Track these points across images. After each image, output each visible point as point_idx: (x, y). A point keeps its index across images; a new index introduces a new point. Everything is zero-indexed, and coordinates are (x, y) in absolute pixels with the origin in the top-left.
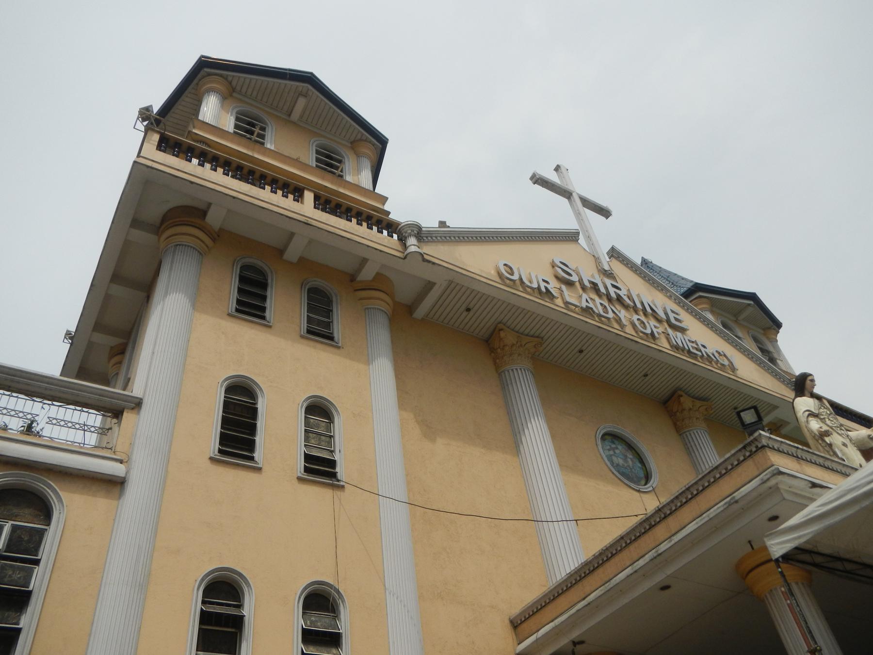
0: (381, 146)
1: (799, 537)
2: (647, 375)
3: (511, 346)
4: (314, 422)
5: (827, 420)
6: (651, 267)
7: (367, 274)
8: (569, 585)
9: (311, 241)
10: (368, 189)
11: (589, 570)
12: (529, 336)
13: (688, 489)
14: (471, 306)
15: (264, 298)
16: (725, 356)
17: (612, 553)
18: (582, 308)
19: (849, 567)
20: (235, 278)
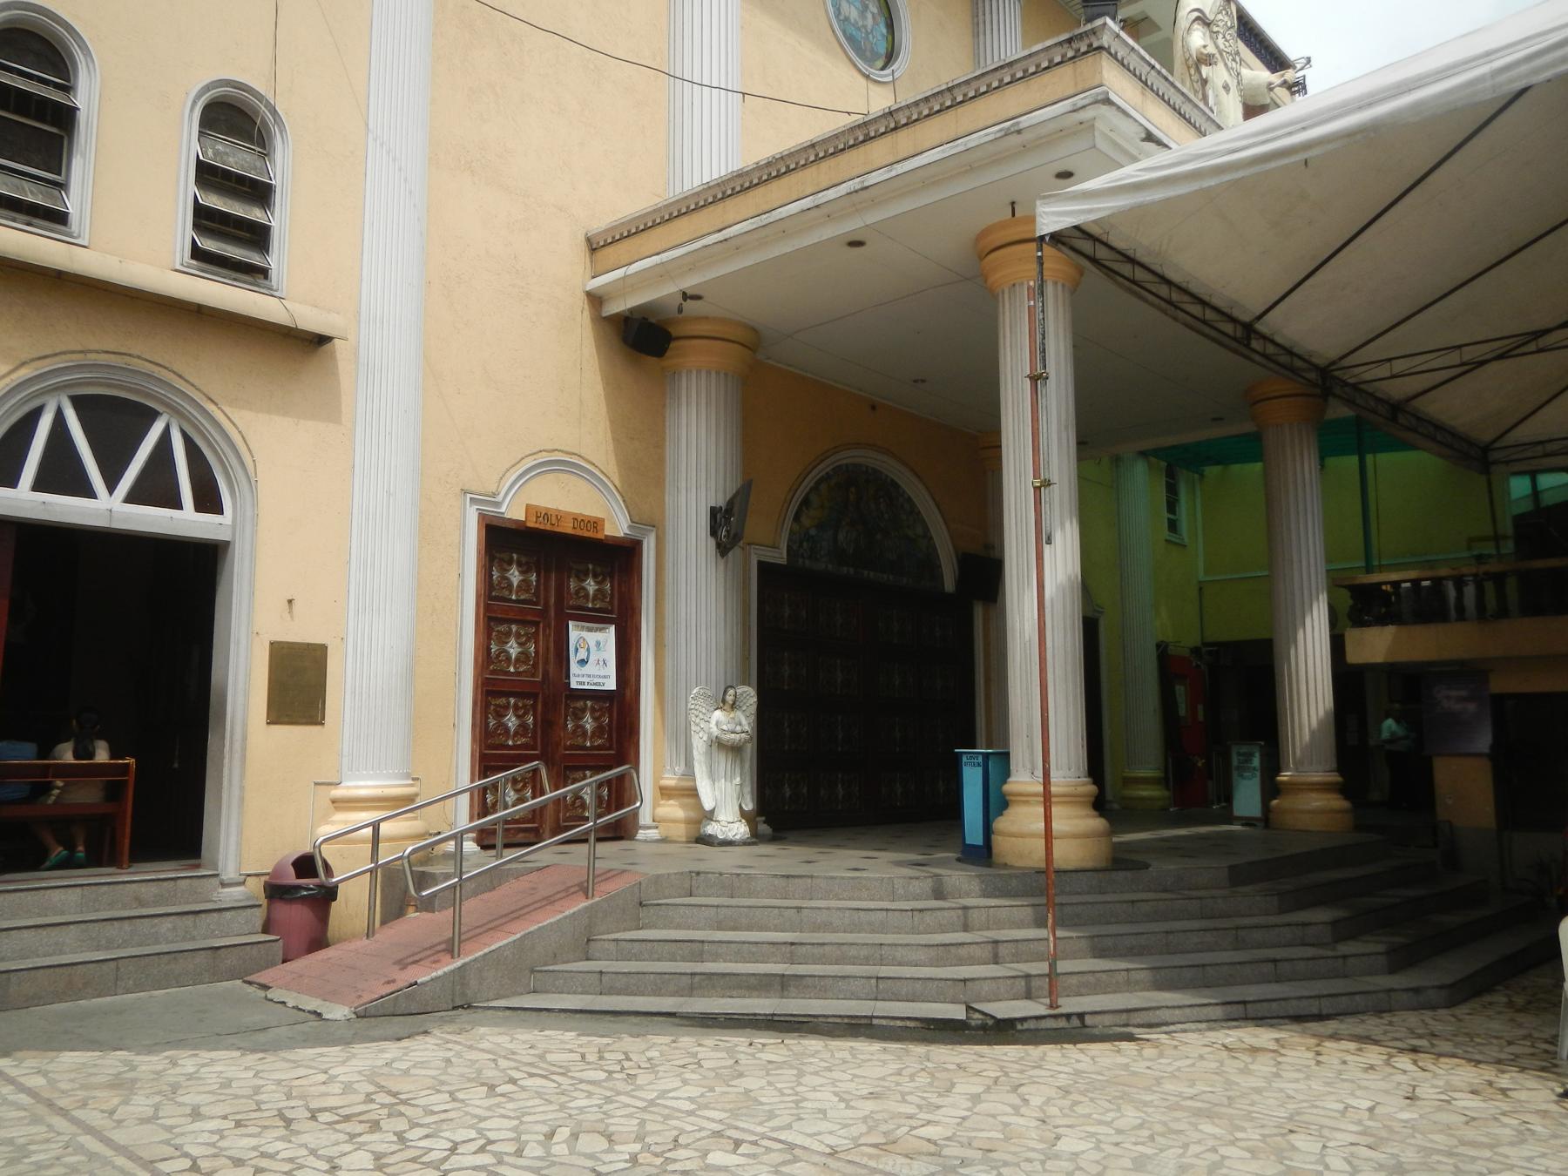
1: (1090, 211)
5: (1220, 36)
8: (702, 203)
11: (742, 186)
13: (950, 89)
17: (788, 167)
19: (1140, 275)
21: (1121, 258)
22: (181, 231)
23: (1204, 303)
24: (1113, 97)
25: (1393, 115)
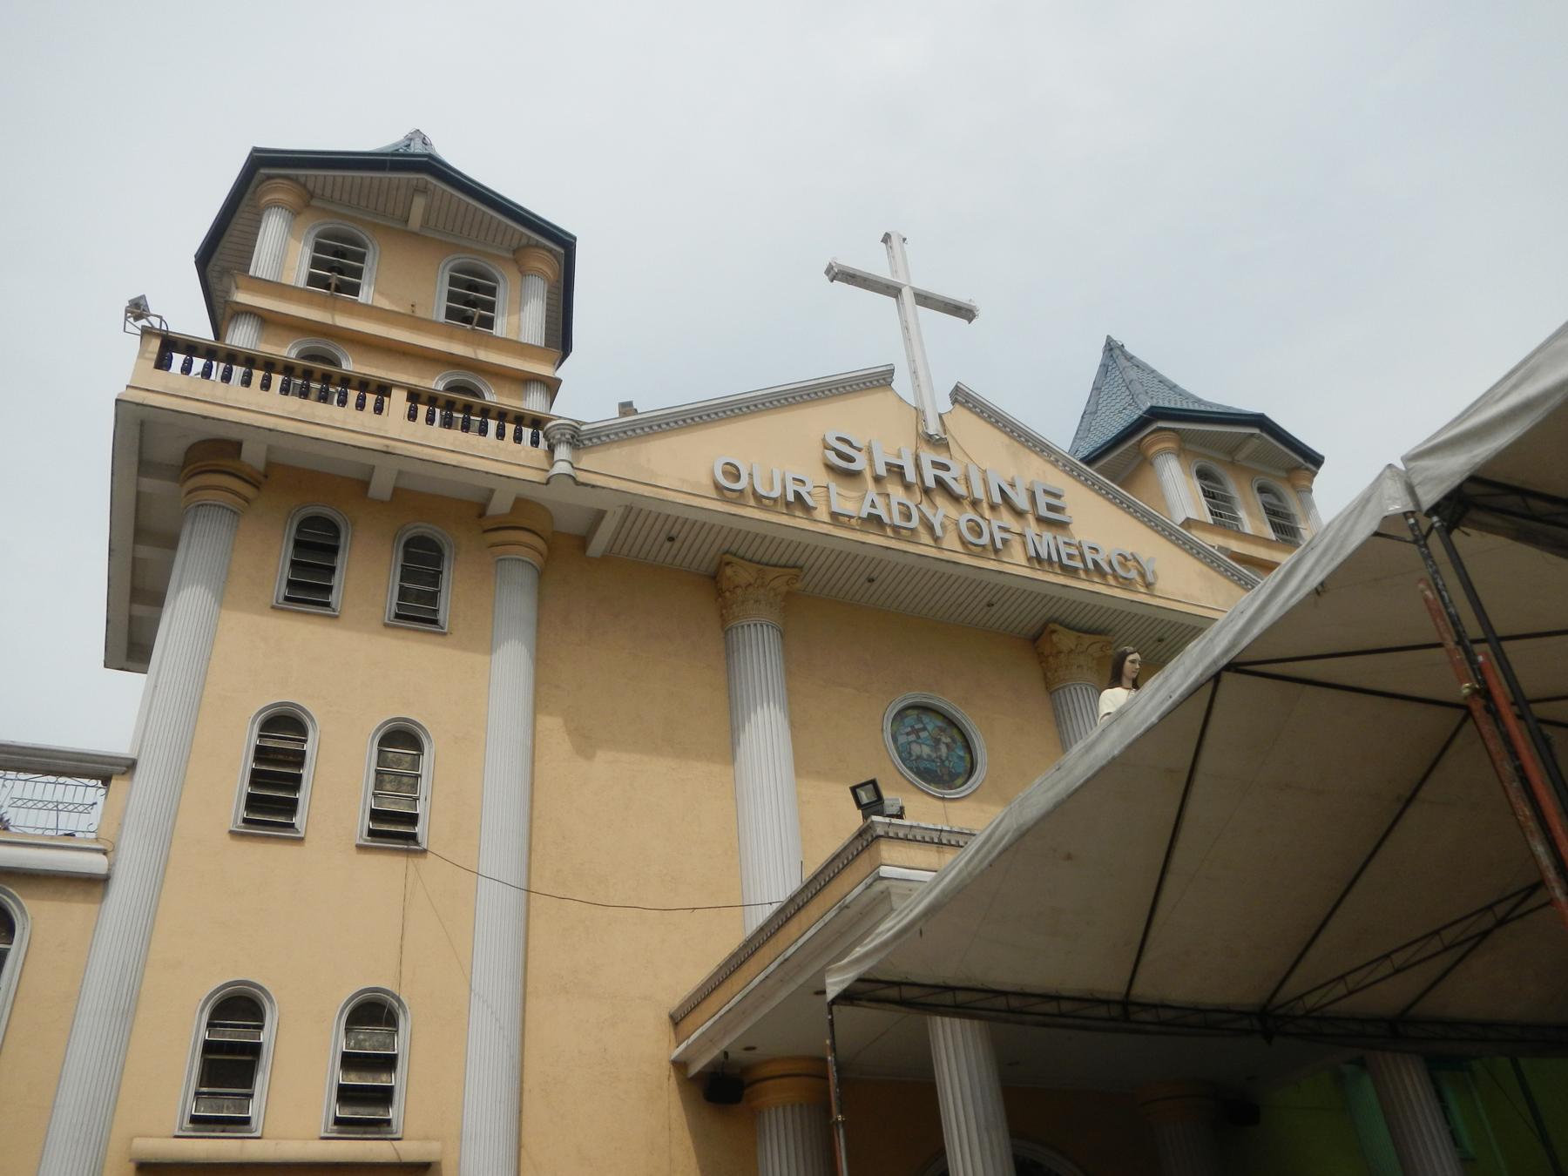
0: (563, 252)
1: (843, 981)
2: (993, 605)
3: (746, 588)
4: (394, 756)
6: (1114, 356)
7: (500, 505)
9: (400, 473)
10: (526, 344)
12: (780, 567)
14: (673, 533)
15: (332, 570)
16: (1135, 558)
18: (860, 518)
19: (961, 997)
20: (287, 544)
21: (937, 990)
22: (325, 1107)
23: (1057, 998)
24: (881, 875)
25: (936, 898)
